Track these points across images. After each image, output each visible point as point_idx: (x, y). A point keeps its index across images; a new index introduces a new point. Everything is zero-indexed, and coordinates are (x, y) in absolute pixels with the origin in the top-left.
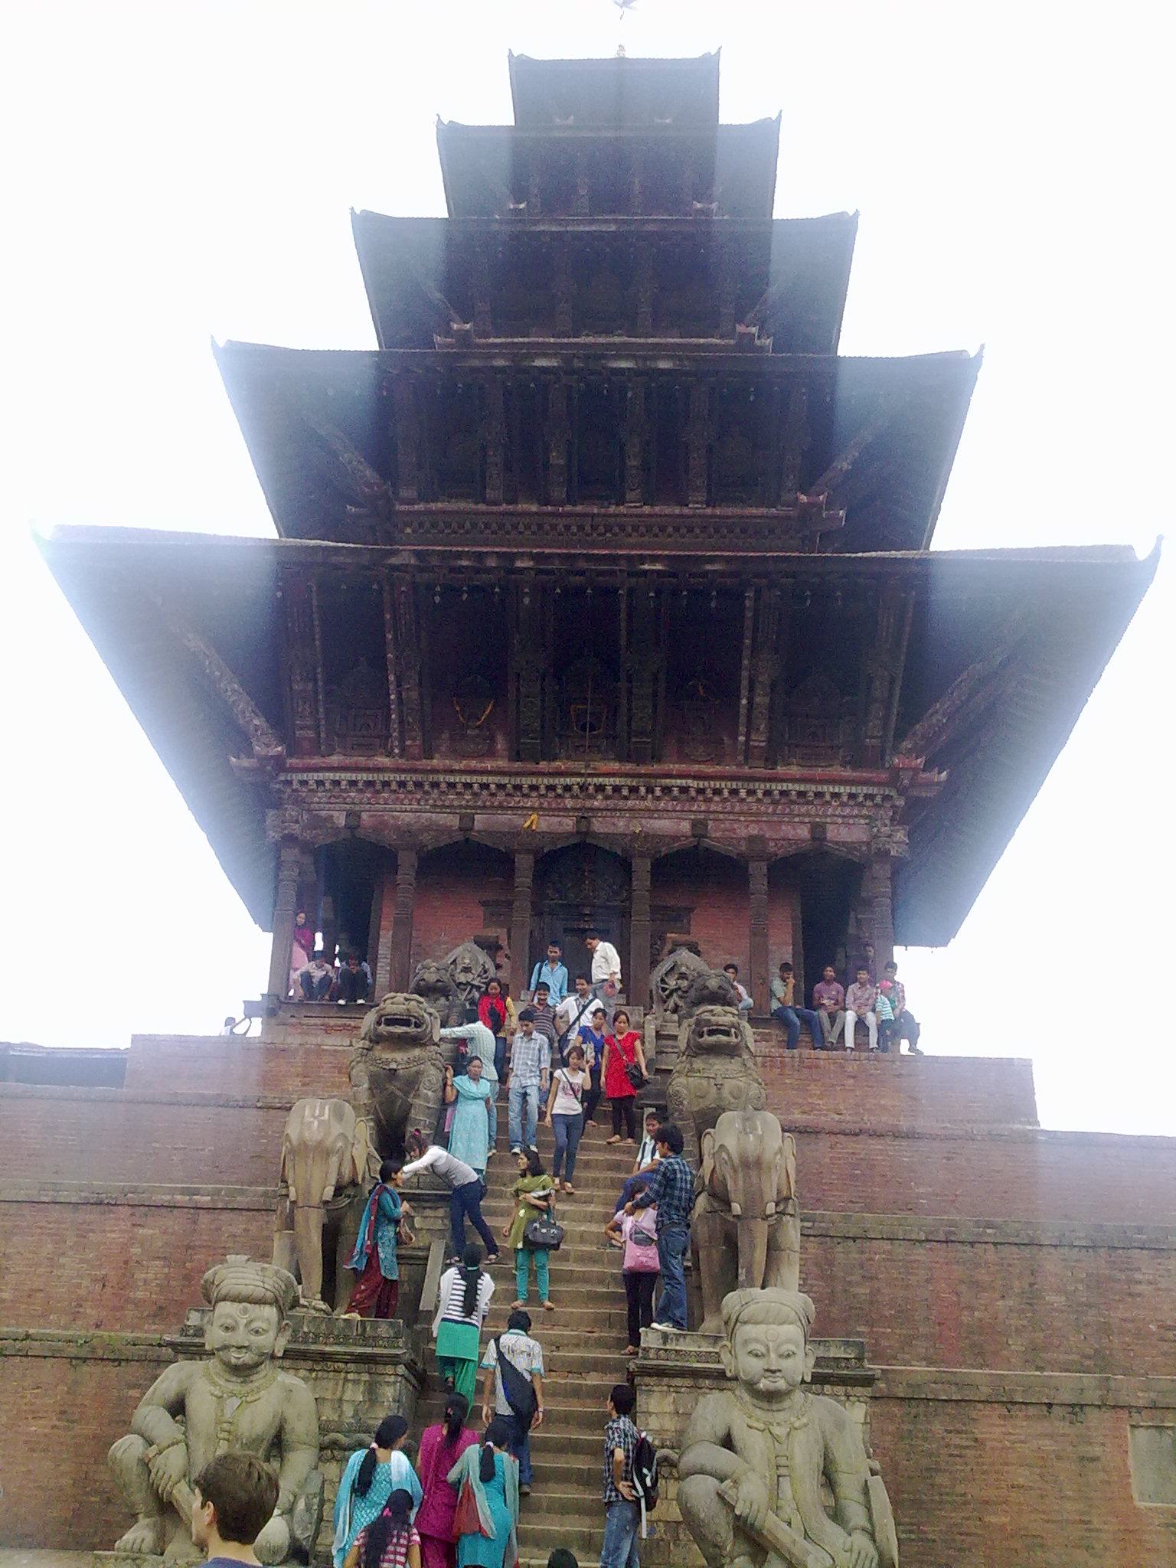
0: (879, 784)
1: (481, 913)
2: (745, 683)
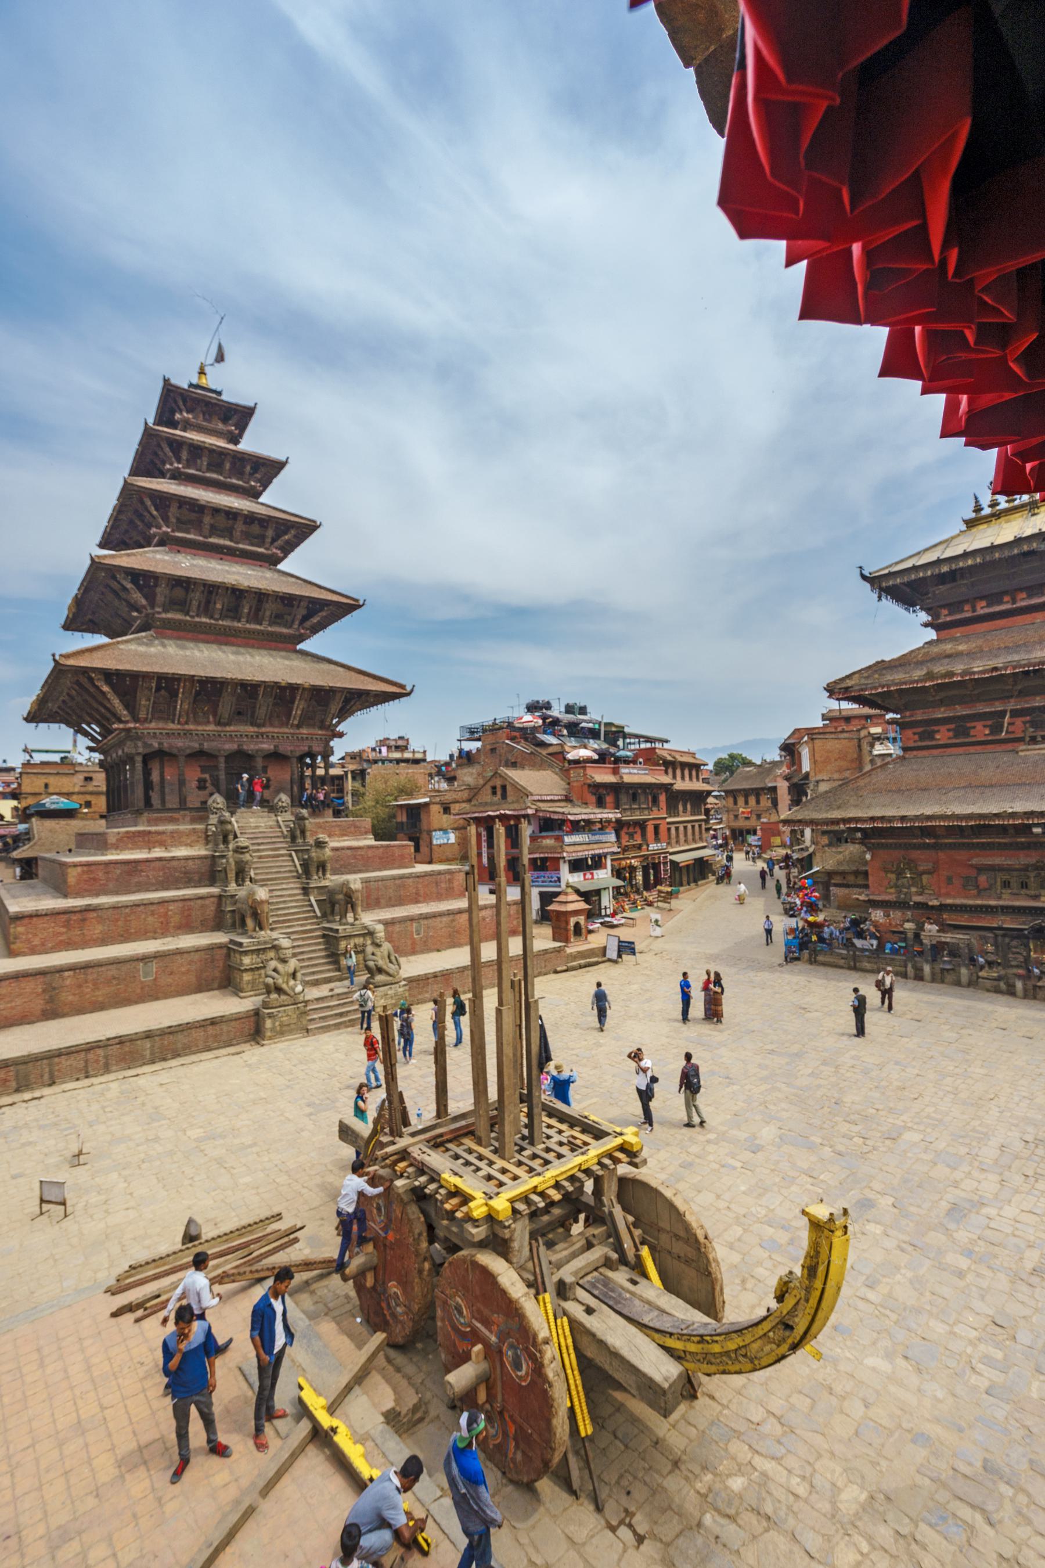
1: (199, 769)
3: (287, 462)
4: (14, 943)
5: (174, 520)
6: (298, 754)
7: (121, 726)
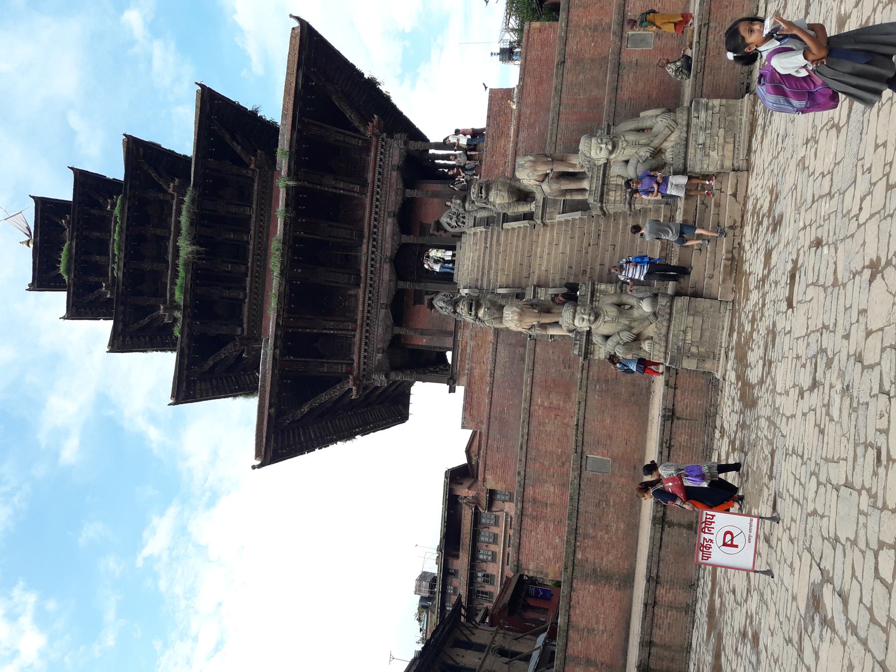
0: (377, 142)
1: (418, 306)
2: (334, 191)
3: (72, 168)
4: (547, 575)
5: (152, 301)
6: (401, 186)
7: (354, 392)
